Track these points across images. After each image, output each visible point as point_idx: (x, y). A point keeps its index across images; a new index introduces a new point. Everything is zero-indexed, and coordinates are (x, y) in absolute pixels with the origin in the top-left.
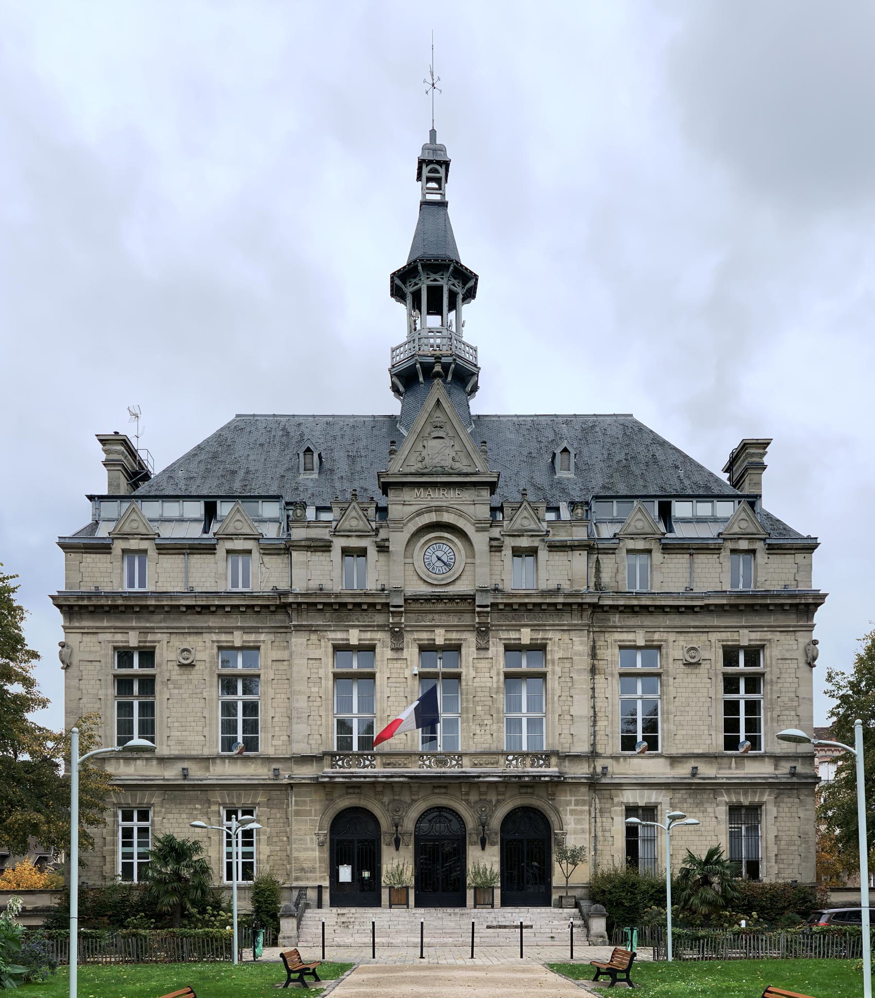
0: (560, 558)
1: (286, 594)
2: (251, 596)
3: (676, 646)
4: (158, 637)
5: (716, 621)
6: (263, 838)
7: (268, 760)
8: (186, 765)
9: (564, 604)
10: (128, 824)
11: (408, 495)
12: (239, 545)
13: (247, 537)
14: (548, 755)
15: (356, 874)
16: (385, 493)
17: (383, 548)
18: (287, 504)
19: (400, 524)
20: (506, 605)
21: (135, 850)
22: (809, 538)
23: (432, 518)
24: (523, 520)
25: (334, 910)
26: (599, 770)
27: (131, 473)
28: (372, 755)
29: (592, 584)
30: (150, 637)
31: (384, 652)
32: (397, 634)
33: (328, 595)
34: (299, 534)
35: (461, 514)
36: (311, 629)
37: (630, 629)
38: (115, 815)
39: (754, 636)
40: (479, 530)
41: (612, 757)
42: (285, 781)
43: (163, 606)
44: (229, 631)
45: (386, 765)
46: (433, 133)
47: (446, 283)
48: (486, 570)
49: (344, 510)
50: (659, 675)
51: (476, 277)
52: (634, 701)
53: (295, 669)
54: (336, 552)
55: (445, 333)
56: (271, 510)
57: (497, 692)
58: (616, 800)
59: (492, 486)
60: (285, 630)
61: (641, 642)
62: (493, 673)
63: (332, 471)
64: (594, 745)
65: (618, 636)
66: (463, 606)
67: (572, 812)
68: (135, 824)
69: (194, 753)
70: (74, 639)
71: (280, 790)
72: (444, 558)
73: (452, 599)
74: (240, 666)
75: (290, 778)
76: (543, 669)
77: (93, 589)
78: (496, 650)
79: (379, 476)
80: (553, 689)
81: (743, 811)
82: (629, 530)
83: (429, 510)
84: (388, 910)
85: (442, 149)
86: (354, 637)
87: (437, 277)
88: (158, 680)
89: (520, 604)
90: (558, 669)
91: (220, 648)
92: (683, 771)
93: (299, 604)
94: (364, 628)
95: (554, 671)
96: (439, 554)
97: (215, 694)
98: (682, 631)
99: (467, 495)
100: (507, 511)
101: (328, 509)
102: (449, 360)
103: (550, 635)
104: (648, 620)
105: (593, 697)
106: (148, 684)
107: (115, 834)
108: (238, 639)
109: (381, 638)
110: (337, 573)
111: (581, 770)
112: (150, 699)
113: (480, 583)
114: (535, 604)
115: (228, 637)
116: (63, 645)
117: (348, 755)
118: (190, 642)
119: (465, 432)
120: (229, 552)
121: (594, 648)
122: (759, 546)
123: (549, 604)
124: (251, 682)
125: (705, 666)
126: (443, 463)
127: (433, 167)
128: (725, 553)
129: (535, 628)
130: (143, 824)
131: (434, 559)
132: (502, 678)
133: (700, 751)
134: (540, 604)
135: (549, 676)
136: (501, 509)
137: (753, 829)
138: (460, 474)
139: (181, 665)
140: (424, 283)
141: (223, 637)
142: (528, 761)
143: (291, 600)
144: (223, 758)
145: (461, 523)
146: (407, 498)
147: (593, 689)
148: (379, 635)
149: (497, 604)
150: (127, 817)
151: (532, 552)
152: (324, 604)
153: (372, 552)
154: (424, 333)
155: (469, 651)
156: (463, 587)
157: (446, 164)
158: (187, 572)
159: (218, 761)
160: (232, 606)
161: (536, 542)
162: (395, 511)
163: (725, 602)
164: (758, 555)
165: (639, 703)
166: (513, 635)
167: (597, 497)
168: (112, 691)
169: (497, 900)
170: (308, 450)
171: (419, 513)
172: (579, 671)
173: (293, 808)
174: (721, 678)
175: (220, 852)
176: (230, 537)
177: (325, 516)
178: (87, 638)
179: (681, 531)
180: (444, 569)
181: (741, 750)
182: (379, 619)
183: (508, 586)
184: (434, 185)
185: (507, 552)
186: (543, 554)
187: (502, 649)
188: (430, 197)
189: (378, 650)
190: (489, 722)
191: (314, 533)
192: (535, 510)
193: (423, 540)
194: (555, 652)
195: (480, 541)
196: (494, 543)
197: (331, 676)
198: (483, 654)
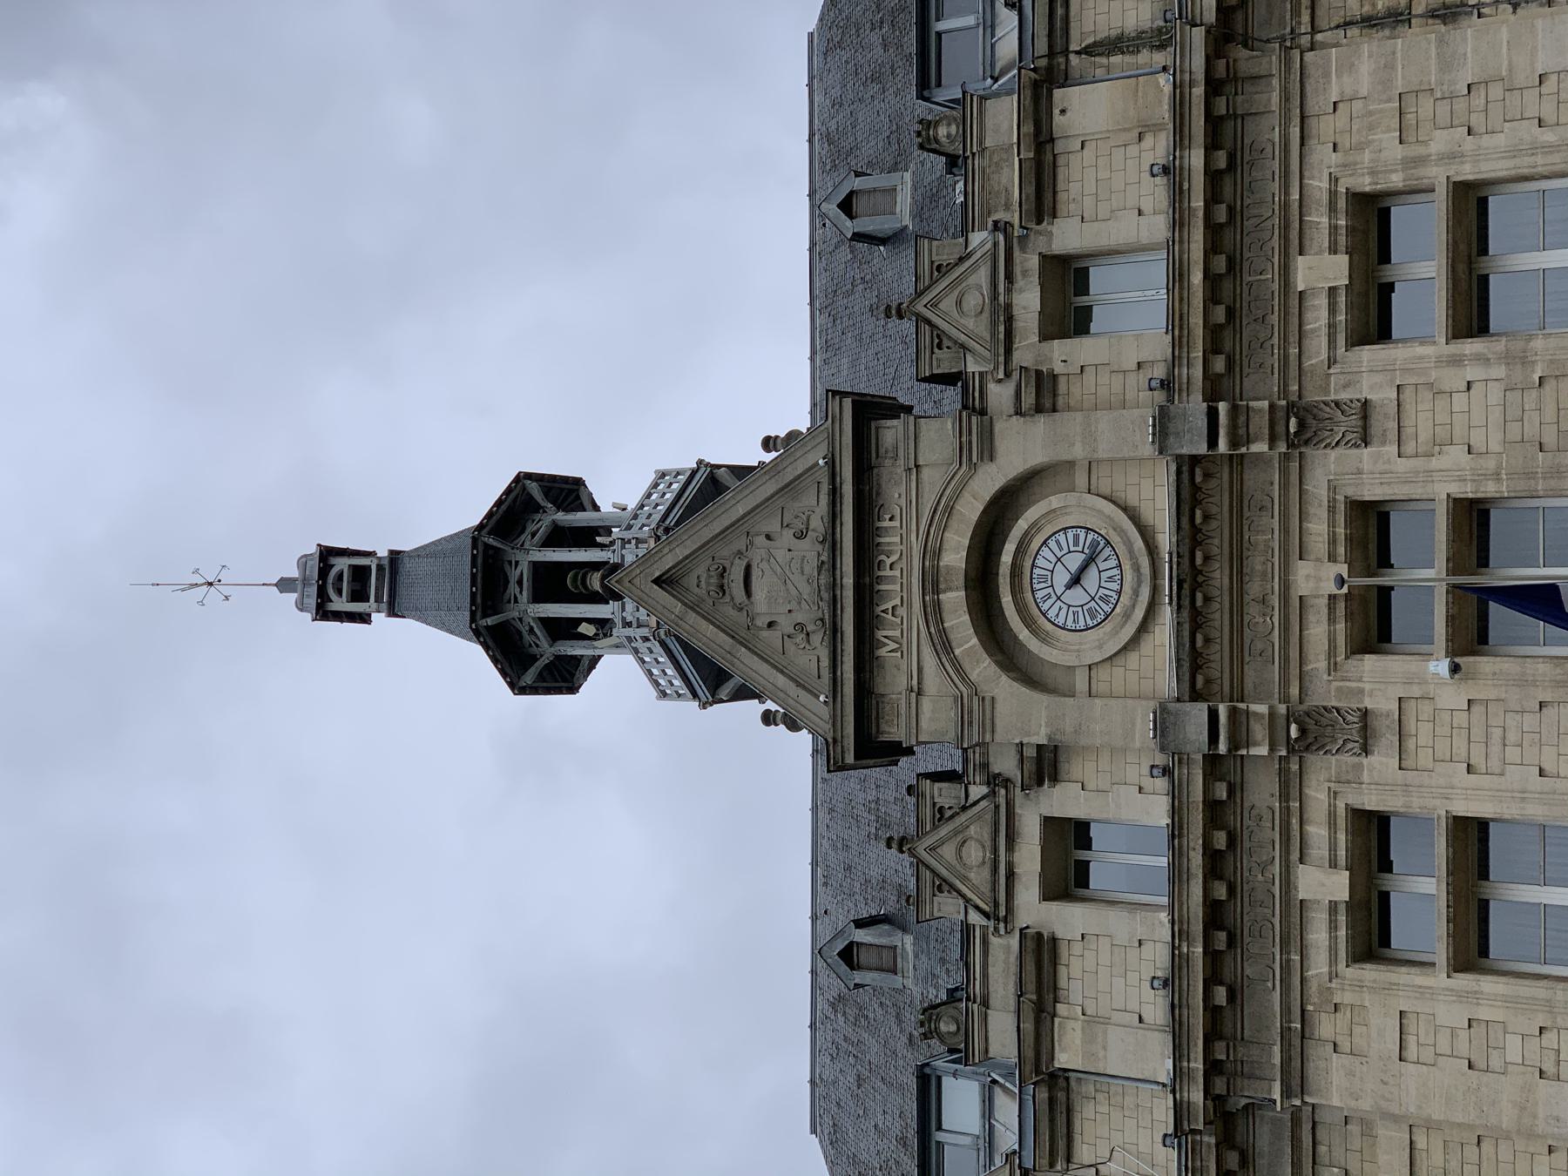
0: (1080, 178)
1: (1181, 1111)
9: (1211, 147)
16: (894, 752)
17: (1046, 765)
24: (964, 310)
29: (1160, 58)
31: (1377, 782)
32: (1310, 732)
33: (1178, 962)
35: (945, 511)
36: (1298, 1039)
48: (1104, 422)
53: (1437, 1112)
54: (1066, 919)
57: (1525, 361)
62: (1453, 379)
66: (1219, 503)
72: (1074, 562)
73: (1191, 533)
78: (1369, 373)
80: (1514, 152)
83: (933, 612)
86: (1324, 884)
89: (1212, 298)
90: (1439, 142)
93: (1213, 1068)
94: (1294, 847)
95: (1452, 155)
96: (1062, 578)
99: (895, 492)
103: (1319, 185)
109: (1332, 788)
110: (1118, 923)
113: (1147, 449)
114: (1212, 249)
121: (1370, 22)
126: (811, 567)
129: (1294, 241)
131: (1076, 596)
135: (1467, 172)
138: (834, 515)
143: (1197, 1096)
145: (971, 509)
146: (902, 682)
148: (1317, 795)
153: (1063, 801)
155: (1371, 472)
156: (1157, 499)
166: (1318, 317)
167: (924, 86)
171: (943, 645)
172: (1446, 65)
180: (1106, 563)
182: (1262, 791)
185: (1062, 354)
186: (1066, 236)
189: (1371, 802)
193: (1023, 634)
194: (1378, 161)
195: (1021, 445)
196: (1029, 399)
197: (1464, 981)
198: (1383, 423)
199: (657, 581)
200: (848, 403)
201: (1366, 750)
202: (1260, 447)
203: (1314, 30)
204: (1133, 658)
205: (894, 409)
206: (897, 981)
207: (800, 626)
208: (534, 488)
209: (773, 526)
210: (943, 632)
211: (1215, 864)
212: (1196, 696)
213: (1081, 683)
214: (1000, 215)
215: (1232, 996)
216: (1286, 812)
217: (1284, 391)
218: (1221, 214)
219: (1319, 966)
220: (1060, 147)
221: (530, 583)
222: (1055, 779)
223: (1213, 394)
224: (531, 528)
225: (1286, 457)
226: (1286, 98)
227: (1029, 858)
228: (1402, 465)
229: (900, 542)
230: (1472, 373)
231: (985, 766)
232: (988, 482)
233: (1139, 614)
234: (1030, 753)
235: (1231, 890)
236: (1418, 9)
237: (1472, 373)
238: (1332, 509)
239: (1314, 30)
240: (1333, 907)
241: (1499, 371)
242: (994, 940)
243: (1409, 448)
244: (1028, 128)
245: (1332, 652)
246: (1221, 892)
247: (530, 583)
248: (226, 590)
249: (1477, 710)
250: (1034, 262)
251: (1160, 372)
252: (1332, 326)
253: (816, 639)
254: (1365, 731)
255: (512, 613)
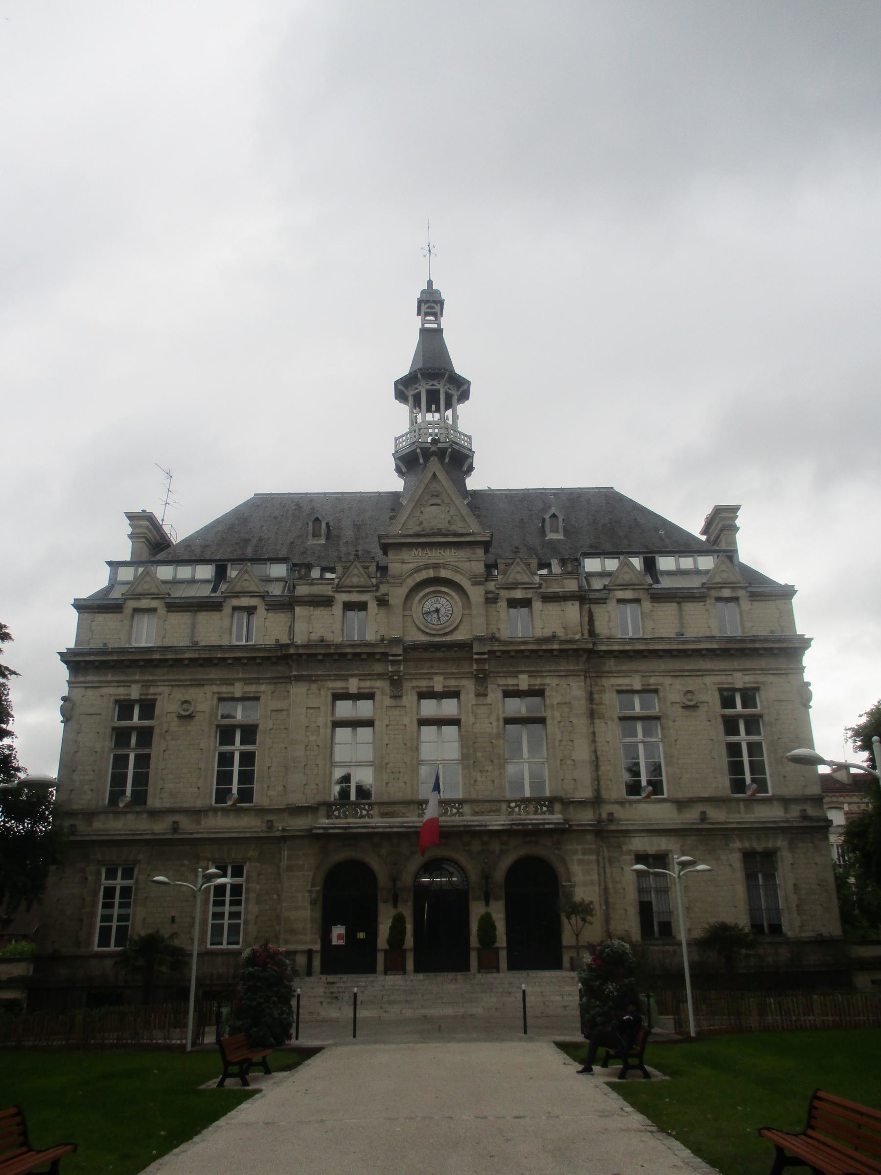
0: (553, 609)
1: (287, 646)
2: (253, 648)
3: (674, 690)
4: (160, 689)
5: (708, 665)
6: (253, 895)
7: (261, 811)
8: (177, 818)
9: (560, 650)
10: (111, 883)
11: (406, 555)
12: (245, 602)
13: (252, 594)
14: (551, 801)
15: (350, 936)
16: (385, 553)
17: (383, 602)
18: (295, 565)
19: (399, 580)
20: (503, 652)
21: (116, 911)
22: (786, 585)
23: (431, 573)
25: (324, 978)
26: (604, 816)
27: (151, 539)
28: (370, 805)
29: (586, 632)
30: (152, 690)
33: (328, 646)
34: (302, 590)
35: (457, 570)
36: (309, 679)
37: (627, 674)
38: (99, 873)
39: (747, 679)
40: (475, 584)
41: (617, 802)
42: (278, 834)
43: (166, 660)
44: (230, 682)
45: (383, 815)
46: (430, 283)
47: (441, 387)
49: (346, 569)
50: (657, 718)
51: (469, 383)
52: (635, 746)
54: (338, 609)
55: (442, 424)
56: (279, 570)
58: (625, 848)
59: (487, 546)
60: (288, 680)
61: (637, 686)
63: (338, 537)
64: (598, 791)
65: (613, 681)
67: (580, 862)
68: (119, 882)
69: (186, 805)
70: (79, 692)
71: (270, 844)
74: (240, 714)
75: (284, 830)
76: (543, 714)
77: (101, 646)
79: (380, 537)
81: (758, 858)
82: (618, 582)
83: (427, 567)
84: (382, 978)
85: (438, 292)
87: (435, 382)
88: (156, 732)
91: (221, 699)
92: (691, 816)
93: (300, 655)
94: (363, 677)
95: (553, 717)
97: (211, 744)
98: (677, 675)
99: (462, 554)
100: (501, 566)
101: (332, 570)
102: (447, 445)
103: (548, 681)
104: (644, 665)
105: (594, 741)
106: (146, 736)
107: (95, 894)
108: (238, 690)
110: (338, 626)
111: (586, 817)
112: (147, 751)
115: (228, 689)
116: (64, 699)
117: (347, 804)
118: (192, 694)
119: (462, 504)
120: (235, 608)
122: (741, 593)
123: (546, 651)
124: (250, 733)
125: (703, 709)
127: (430, 304)
128: (709, 601)
129: (532, 674)
130: (128, 883)
132: (501, 723)
133: (706, 795)
134: (536, 651)
135: (549, 721)
136: (495, 566)
137: (770, 876)
138: (456, 535)
139: (181, 717)
140: (423, 389)
141: (224, 689)
142: (531, 808)
144: (215, 810)
145: (457, 578)
147: (594, 733)
148: (379, 683)
149: (494, 652)
150: (111, 874)
151: (526, 603)
152: (325, 655)
154: (423, 425)
156: (460, 636)
157: (441, 303)
158: (194, 626)
159: (210, 814)
160: (235, 659)
161: (529, 594)
162: (395, 568)
163: (715, 646)
164: (742, 602)
165: (641, 746)
166: (511, 681)
168: (109, 743)
169: (503, 964)
170: (317, 519)
171: (418, 570)
173: (284, 863)
174: (720, 720)
175: (205, 912)
176: (237, 595)
177: (329, 575)
178: (90, 692)
179: (666, 583)
181: (749, 793)
182: (378, 668)
183: (505, 634)
184: (432, 318)
185: (503, 604)
186: (537, 605)
187: (500, 695)
188: (427, 326)
190: (490, 768)
191: (316, 590)
192: (528, 565)
193: (421, 594)
194: (553, 697)
195: (476, 594)
196: (490, 596)
198: (481, 700)
199: (434, 474)
200: (489, 539)
201: (391, 697)
202: (475, 667)
203: (591, 677)
204: (415, 629)
205: (487, 552)
206: (310, 537)
207: (421, 523)
208: (465, 387)
209: (452, 512)
210: (421, 570)
211: (357, 655)
212: (405, 649)
213: (407, 613)
214: (544, 586)
215: (320, 660)
216: (373, 675)
217: (491, 672)
218: (540, 653)
219: (331, 685)
220: (563, 603)
221: (433, 382)
222: (379, 605)
223: (490, 652)
224: (451, 386)
225: (472, 673)
226: (573, 671)
227: (355, 597)
228: (470, 705)
229: (448, 555)
230: (494, 724)
231: (382, 583)
232: (466, 584)
233: (428, 631)
234: (386, 598)
235: (349, 660)
236: (594, 706)
237: (494, 724)
238: (457, 686)
239: (591, 677)
240: (347, 688)
241: (495, 731)
242: (330, 587)
243: (475, 708)
244: (568, 594)
245: (418, 687)
246: (350, 657)
247: (433, 382)
248: (427, 256)
249: (403, 727)
250: (529, 596)
251: (497, 635)
252: (508, 685)
253: (418, 528)
254: (396, 697)
255: (423, 383)
